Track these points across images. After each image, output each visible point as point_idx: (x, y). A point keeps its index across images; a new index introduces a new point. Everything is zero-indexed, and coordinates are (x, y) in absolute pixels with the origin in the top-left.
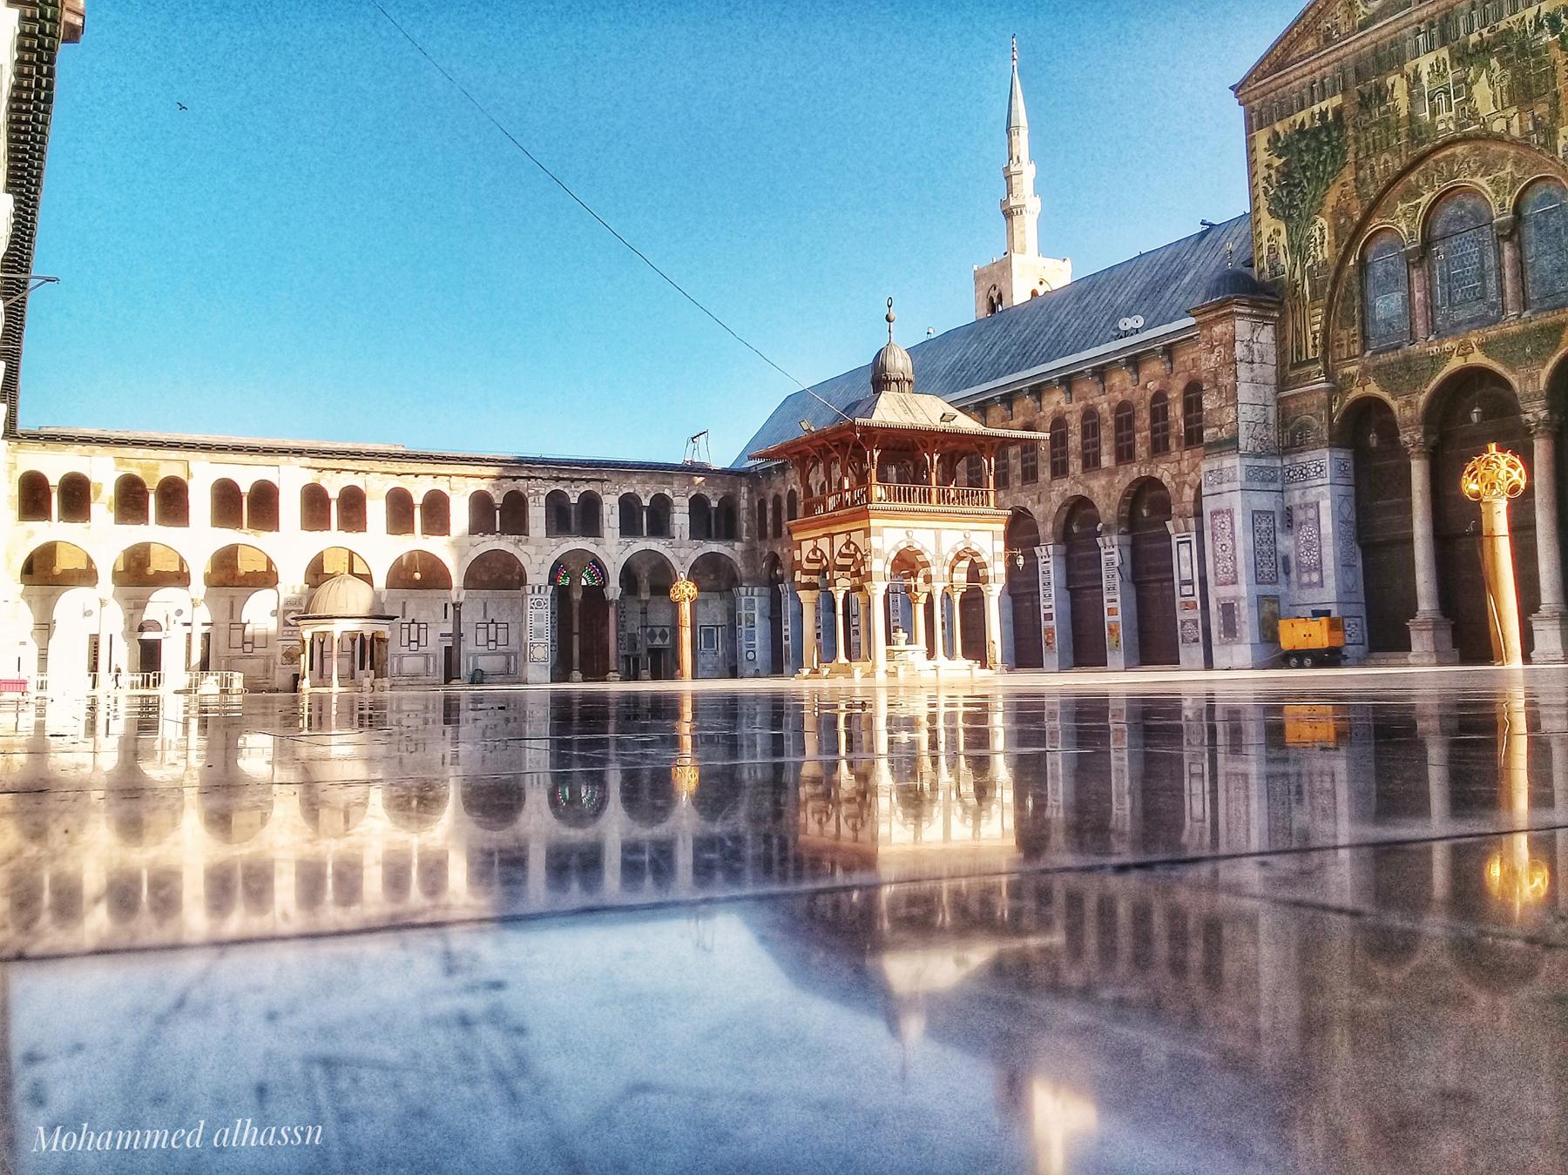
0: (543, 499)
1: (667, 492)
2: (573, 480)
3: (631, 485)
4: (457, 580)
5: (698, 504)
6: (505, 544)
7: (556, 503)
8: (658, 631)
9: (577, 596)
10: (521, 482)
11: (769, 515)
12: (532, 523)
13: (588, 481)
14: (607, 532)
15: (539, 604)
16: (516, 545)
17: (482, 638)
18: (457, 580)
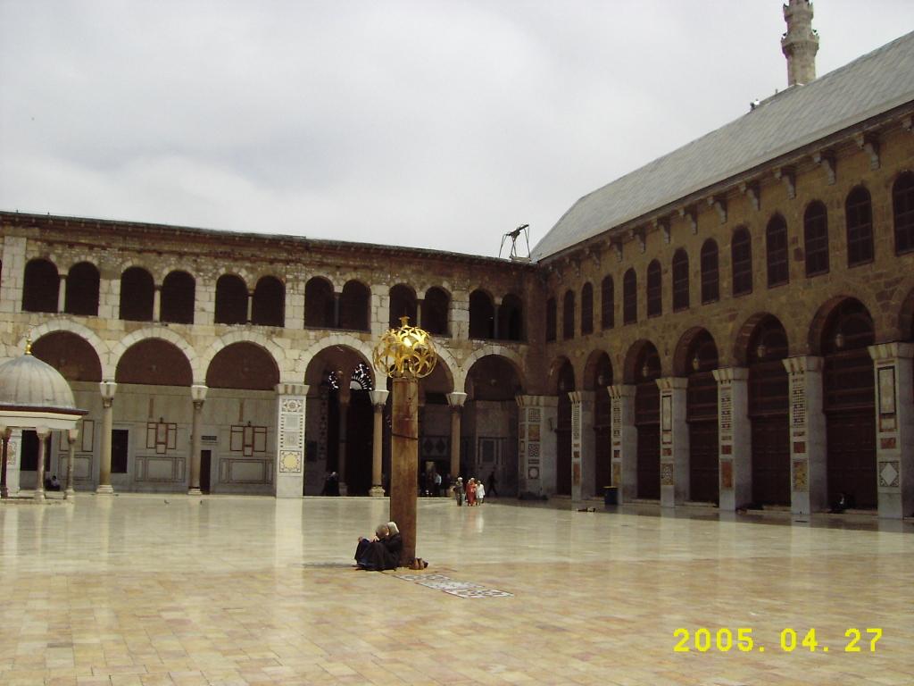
0: (302, 286)
1: (445, 285)
2: (338, 267)
3: (405, 275)
4: (200, 370)
5: (479, 304)
6: (255, 335)
7: (317, 293)
8: (435, 441)
9: (345, 399)
10: (280, 268)
11: (560, 314)
12: (288, 312)
13: (355, 269)
14: (374, 326)
15: (292, 406)
16: (269, 336)
17: (237, 444)
18: (200, 370)
